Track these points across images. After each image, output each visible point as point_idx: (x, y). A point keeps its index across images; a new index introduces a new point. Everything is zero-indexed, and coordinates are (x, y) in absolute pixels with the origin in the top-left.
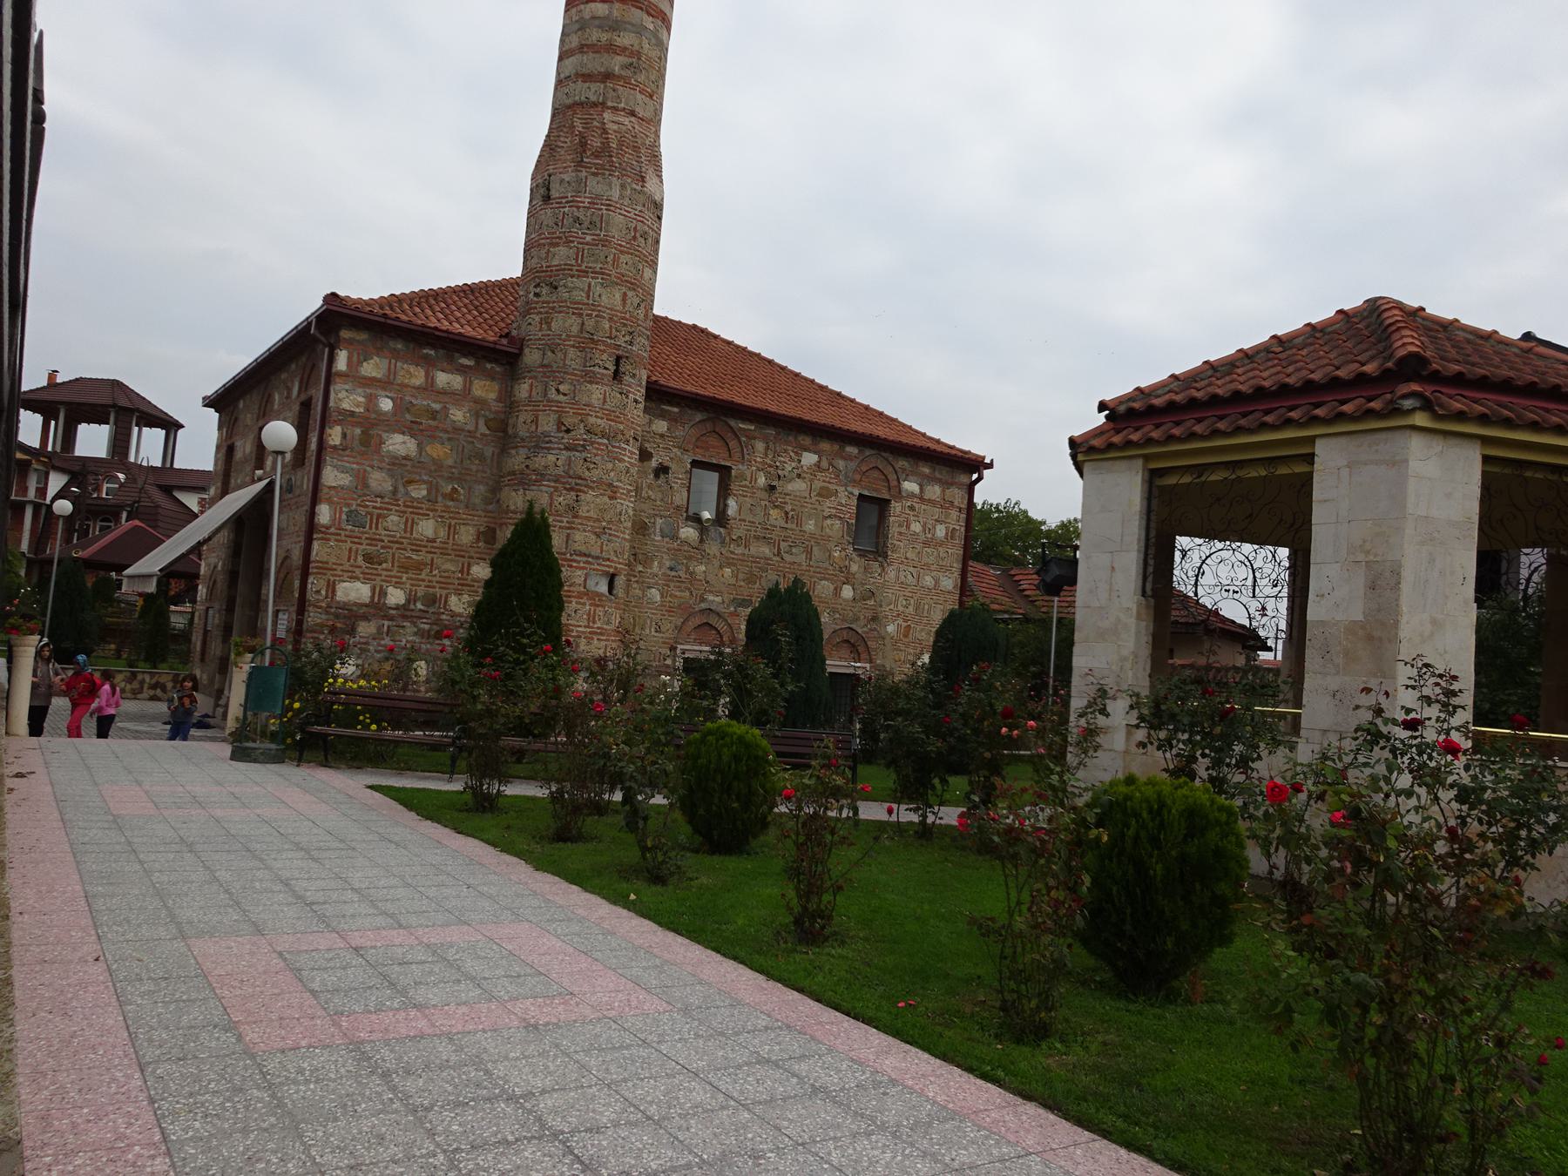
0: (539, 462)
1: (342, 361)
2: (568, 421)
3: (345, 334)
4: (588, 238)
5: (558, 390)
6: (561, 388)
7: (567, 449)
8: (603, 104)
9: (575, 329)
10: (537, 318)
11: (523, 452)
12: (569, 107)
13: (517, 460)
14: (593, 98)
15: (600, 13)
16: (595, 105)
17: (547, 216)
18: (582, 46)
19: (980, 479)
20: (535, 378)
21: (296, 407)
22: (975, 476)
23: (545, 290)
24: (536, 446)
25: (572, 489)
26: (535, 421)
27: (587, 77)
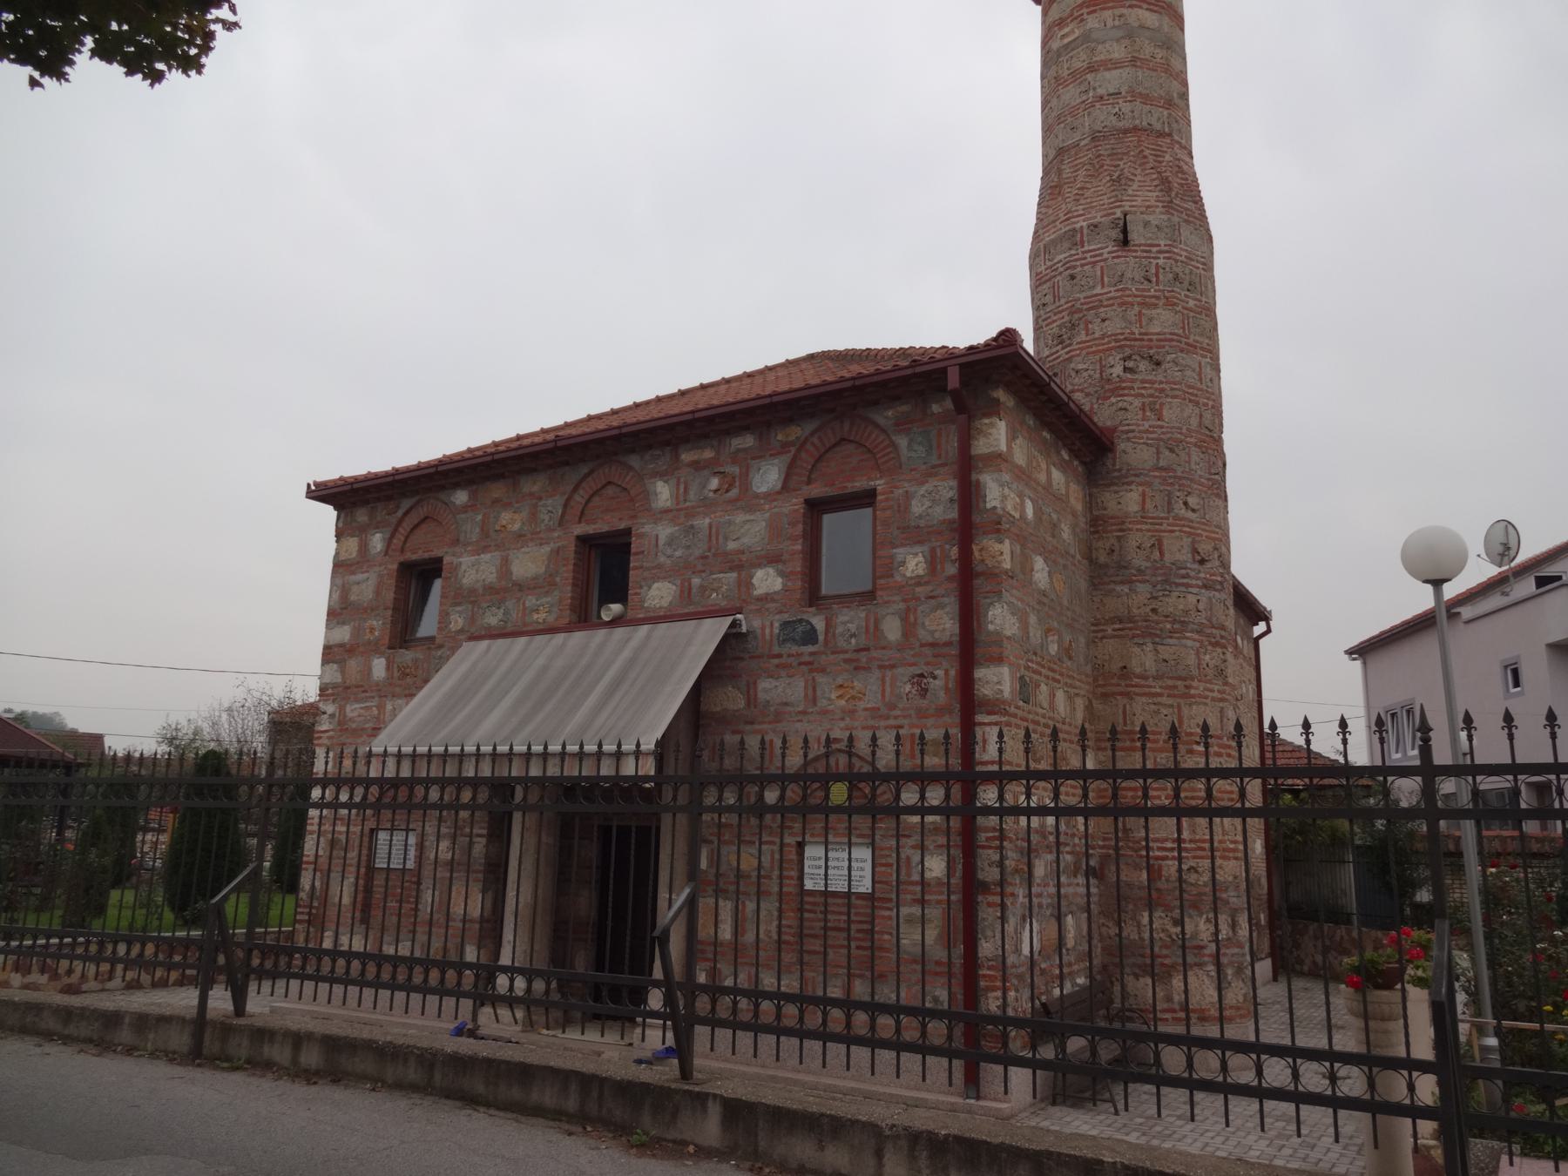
0: (1174, 603)
1: (997, 435)
2: (1205, 547)
3: (1000, 394)
4: (1191, 303)
5: (1185, 503)
6: (1192, 501)
7: (1205, 587)
8: (1170, 135)
9: (1194, 422)
10: (1137, 402)
11: (1143, 589)
12: (1126, 131)
13: (1137, 599)
14: (1158, 126)
15: (1149, 24)
16: (1161, 134)
17: (1129, 265)
18: (1134, 60)
19: (1269, 631)
20: (1149, 484)
21: (793, 505)
22: (1260, 628)
23: (1143, 366)
24: (1166, 581)
25: (1216, 644)
26: (1159, 545)
27: (1146, 99)
